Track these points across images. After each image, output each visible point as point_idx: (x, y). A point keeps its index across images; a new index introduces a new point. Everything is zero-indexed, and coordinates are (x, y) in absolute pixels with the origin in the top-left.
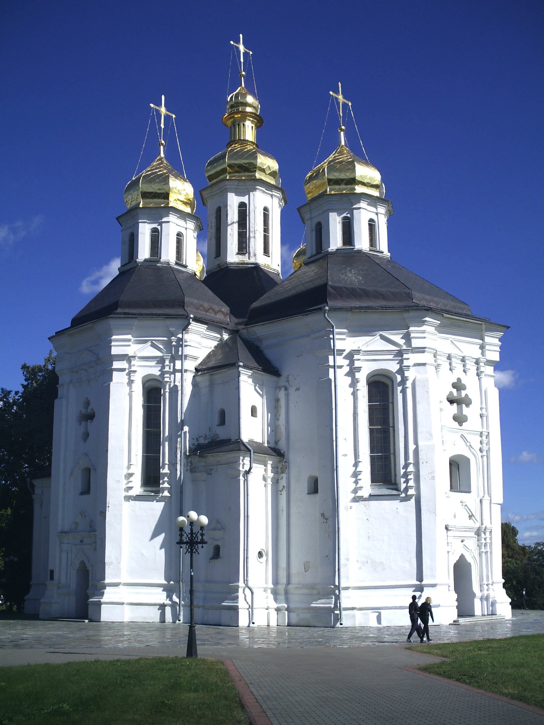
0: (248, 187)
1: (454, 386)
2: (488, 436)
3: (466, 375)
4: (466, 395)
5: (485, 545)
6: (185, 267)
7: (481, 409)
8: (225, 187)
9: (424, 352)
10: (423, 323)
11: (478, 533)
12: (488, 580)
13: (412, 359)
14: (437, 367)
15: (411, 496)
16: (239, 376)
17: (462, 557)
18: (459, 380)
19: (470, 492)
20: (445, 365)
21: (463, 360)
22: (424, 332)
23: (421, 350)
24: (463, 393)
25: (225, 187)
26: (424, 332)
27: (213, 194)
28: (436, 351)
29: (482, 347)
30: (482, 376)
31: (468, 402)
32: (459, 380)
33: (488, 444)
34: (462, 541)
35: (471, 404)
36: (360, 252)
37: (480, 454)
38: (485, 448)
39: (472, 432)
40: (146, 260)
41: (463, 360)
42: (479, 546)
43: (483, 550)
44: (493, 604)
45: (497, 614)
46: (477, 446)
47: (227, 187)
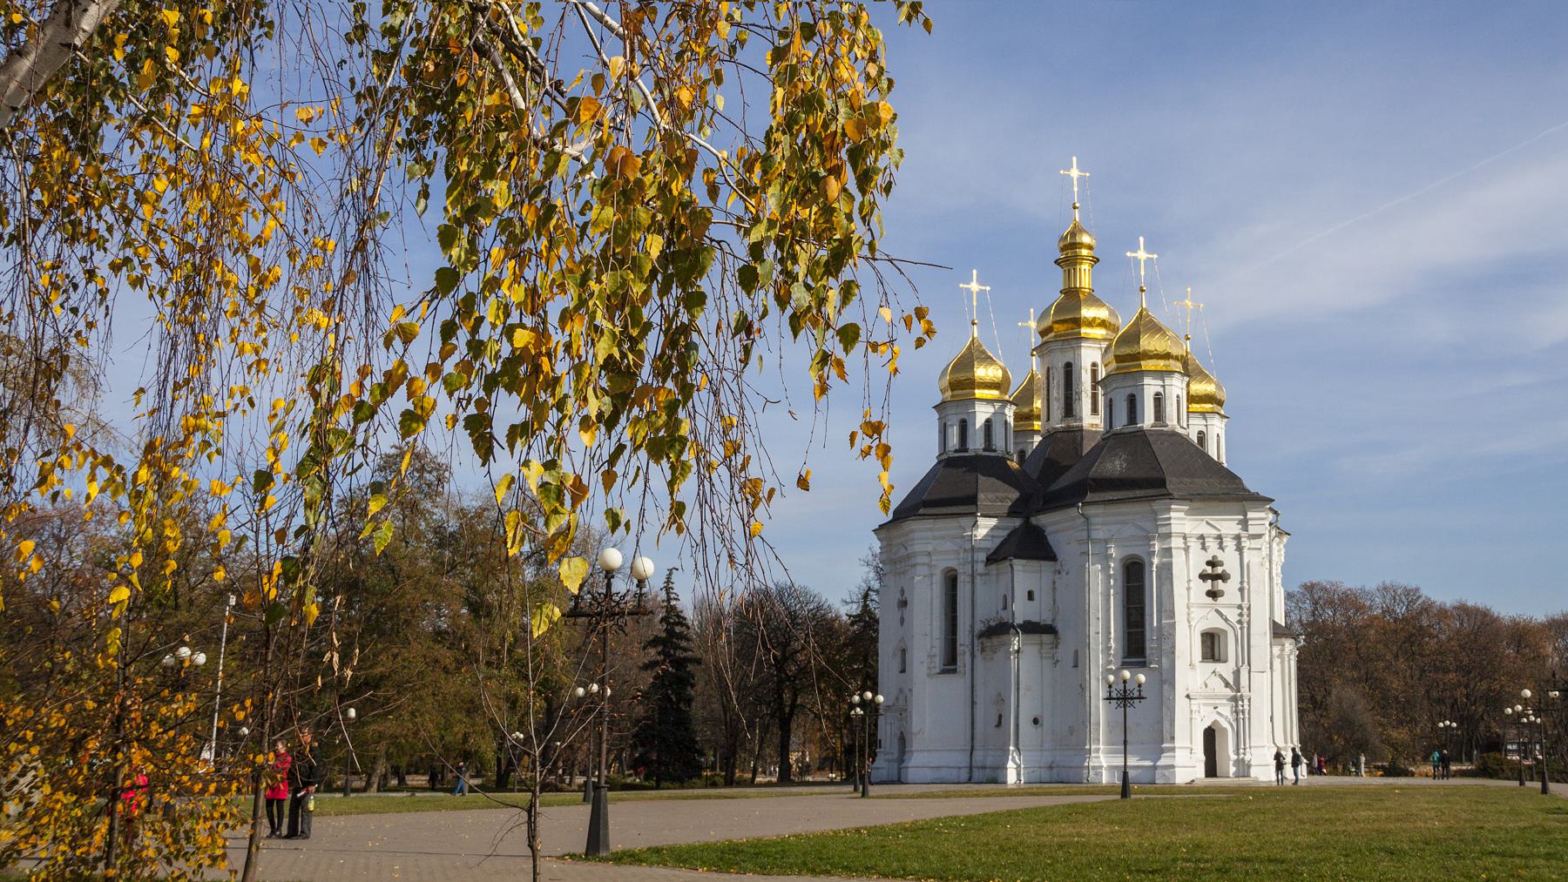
1: (1208, 563)
2: (1249, 609)
5: (1243, 712)
6: (995, 451)
7: (1242, 583)
11: (1235, 699)
14: (1187, 549)
20: (1195, 545)
21: (1220, 537)
22: (1170, 519)
26: (1170, 519)
29: (1244, 524)
30: (1245, 550)
31: (1223, 577)
32: (1214, 557)
33: (1249, 615)
36: (1141, 430)
37: (1238, 626)
38: (1245, 618)
39: (1230, 606)
40: (956, 451)
41: (1220, 537)
42: (1237, 712)
44: (1249, 766)
45: (1252, 775)
46: (1234, 618)
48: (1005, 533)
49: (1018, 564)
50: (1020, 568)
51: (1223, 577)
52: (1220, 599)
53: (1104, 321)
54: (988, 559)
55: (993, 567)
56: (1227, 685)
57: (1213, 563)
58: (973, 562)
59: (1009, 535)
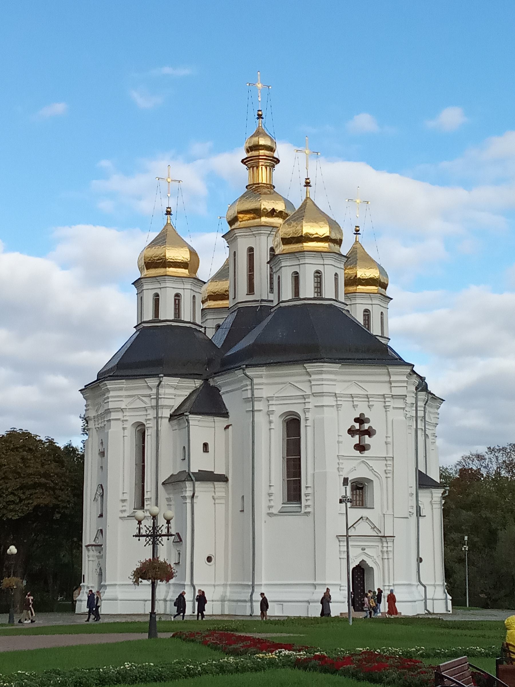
0: (254, 232)
1: (356, 420)
3: (371, 411)
4: (370, 427)
8: (235, 236)
9: (323, 396)
10: (321, 373)
12: (389, 583)
13: (313, 402)
15: (309, 512)
16: (188, 423)
17: (363, 560)
18: (362, 415)
19: (373, 508)
20: (346, 405)
22: (322, 380)
23: (321, 394)
24: (366, 426)
25: (235, 236)
26: (322, 380)
27: (232, 239)
28: (336, 394)
32: (362, 415)
34: (363, 549)
35: (374, 434)
37: (383, 476)
43: (386, 557)
47: (237, 235)
48: (187, 393)
49: (194, 420)
50: (196, 423)
51: (370, 433)
52: (366, 453)
53: (281, 212)
54: (171, 415)
55: (175, 422)
56: (374, 528)
57: (360, 420)
58: (157, 418)
59: (191, 394)
